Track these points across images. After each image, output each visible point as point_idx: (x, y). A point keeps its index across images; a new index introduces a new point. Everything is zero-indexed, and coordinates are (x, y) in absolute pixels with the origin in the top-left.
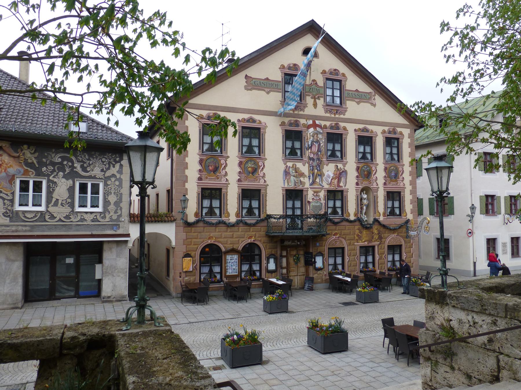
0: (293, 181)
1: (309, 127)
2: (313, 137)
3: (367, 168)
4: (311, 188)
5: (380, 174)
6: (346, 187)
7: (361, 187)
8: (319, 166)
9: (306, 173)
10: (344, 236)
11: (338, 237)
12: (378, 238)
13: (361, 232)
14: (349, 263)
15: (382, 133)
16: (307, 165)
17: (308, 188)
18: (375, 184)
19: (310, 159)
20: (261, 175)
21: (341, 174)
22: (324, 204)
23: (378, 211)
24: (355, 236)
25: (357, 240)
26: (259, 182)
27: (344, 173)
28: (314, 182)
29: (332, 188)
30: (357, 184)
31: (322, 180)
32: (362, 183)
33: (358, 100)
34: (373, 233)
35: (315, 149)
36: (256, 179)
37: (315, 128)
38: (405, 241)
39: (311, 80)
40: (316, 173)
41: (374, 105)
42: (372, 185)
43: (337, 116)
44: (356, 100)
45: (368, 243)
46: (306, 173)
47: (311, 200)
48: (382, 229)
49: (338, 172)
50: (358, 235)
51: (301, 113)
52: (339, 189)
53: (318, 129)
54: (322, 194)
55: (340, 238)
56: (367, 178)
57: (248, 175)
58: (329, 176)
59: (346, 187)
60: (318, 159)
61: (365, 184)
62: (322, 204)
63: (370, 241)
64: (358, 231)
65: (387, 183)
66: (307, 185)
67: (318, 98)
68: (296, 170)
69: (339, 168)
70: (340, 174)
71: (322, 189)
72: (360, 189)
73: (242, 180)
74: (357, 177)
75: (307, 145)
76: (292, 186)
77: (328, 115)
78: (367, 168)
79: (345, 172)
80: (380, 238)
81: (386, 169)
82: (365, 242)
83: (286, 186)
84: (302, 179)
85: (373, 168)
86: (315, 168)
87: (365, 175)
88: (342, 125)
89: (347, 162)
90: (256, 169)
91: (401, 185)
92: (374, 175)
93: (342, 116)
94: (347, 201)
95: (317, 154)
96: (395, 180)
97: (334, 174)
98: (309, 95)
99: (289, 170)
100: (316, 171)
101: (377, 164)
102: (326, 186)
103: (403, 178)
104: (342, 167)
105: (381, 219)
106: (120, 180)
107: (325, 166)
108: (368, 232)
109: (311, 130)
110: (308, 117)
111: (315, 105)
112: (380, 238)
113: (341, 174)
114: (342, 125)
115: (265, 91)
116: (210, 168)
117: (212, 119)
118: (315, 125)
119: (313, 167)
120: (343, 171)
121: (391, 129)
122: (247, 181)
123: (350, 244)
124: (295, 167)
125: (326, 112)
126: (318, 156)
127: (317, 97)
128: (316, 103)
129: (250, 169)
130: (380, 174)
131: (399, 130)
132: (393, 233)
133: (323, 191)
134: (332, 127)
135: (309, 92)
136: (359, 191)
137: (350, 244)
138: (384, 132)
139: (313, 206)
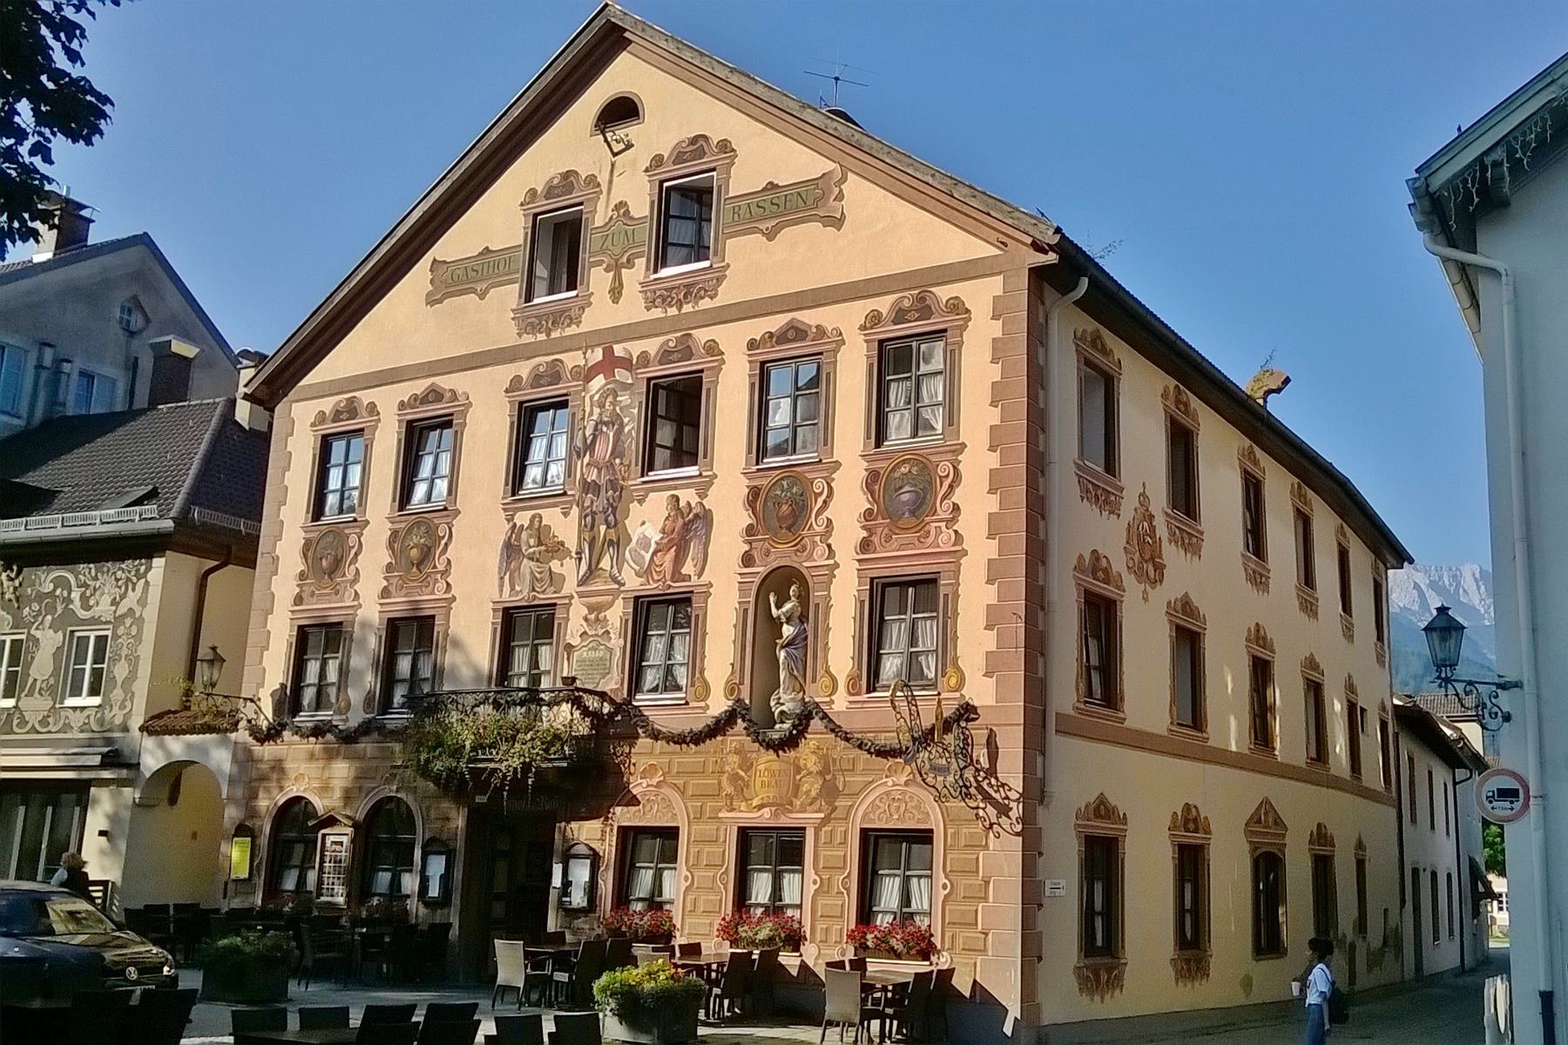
0: (528, 577)
1: (588, 374)
2: (602, 406)
3: (790, 488)
4: (581, 595)
5: (846, 507)
6: (705, 579)
7: (762, 570)
8: (614, 513)
9: (572, 544)
10: (680, 782)
11: (658, 785)
12: (819, 795)
13: (747, 765)
14: (690, 898)
15: (863, 328)
16: (575, 511)
17: (572, 597)
18: (821, 549)
19: (588, 487)
20: (441, 567)
21: (689, 529)
22: (618, 653)
23: (828, 671)
24: (724, 778)
25: (730, 797)
26: (433, 593)
27: (699, 524)
28: (592, 572)
29: (653, 588)
30: (747, 560)
31: (619, 562)
32: (768, 554)
33: (770, 224)
34: (798, 770)
35: (603, 449)
36: (426, 582)
37: (609, 374)
38: (945, 814)
39: (612, 206)
40: (603, 532)
41: (837, 222)
42: (810, 558)
43: (687, 308)
44: (763, 226)
45: (775, 815)
46: (572, 544)
47: (575, 641)
48: (840, 749)
49: (680, 521)
50: (735, 778)
51: (572, 330)
52: (679, 587)
53: (621, 375)
54: (617, 614)
55: (667, 791)
56: (789, 529)
57: (408, 571)
58: (644, 543)
59: (705, 579)
60: (613, 484)
61: (781, 555)
62: (611, 650)
63: (782, 806)
64: (734, 759)
65: (875, 539)
66: (570, 587)
67: (630, 264)
68: (541, 533)
69: (682, 504)
70: (687, 527)
71: (615, 594)
72: (757, 580)
73: (392, 588)
74: (750, 531)
75: (579, 443)
76: (520, 595)
77: (657, 313)
78: (790, 488)
79: (705, 517)
80: (830, 792)
81: (872, 478)
82: (761, 807)
83: (506, 596)
84: (555, 565)
85: (819, 485)
86: (600, 518)
87: (779, 519)
88: (702, 336)
89: (715, 476)
90: (429, 549)
91: (945, 540)
92: (819, 513)
93: (706, 304)
94: (705, 634)
95: (610, 465)
96: (914, 521)
97: (663, 531)
98: (600, 263)
99: (518, 538)
100: (603, 528)
101: (837, 465)
102: (633, 582)
103: (956, 508)
104: (694, 501)
105: (840, 703)
106: (139, 621)
107: (634, 506)
108: (776, 766)
109: (598, 382)
110: (584, 342)
111: (616, 293)
112: (830, 792)
113: (689, 529)
114: (702, 336)
115: (474, 291)
116: (324, 563)
117: (344, 416)
118: (610, 363)
119: (594, 514)
120: (697, 516)
121: (908, 298)
122: (404, 592)
123: (699, 816)
124: (536, 524)
125: (651, 304)
126: (614, 473)
127: (624, 260)
128: (621, 284)
129: (414, 553)
130: (846, 507)
131: (944, 293)
132: (891, 772)
133: (619, 602)
134: (666, 356)
135: (603, 251)
136: (754, 588)
137: (699, 816)
138: (875, 319)
139: (581, 661)
